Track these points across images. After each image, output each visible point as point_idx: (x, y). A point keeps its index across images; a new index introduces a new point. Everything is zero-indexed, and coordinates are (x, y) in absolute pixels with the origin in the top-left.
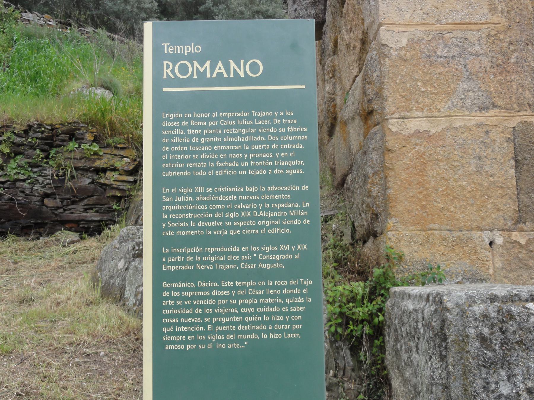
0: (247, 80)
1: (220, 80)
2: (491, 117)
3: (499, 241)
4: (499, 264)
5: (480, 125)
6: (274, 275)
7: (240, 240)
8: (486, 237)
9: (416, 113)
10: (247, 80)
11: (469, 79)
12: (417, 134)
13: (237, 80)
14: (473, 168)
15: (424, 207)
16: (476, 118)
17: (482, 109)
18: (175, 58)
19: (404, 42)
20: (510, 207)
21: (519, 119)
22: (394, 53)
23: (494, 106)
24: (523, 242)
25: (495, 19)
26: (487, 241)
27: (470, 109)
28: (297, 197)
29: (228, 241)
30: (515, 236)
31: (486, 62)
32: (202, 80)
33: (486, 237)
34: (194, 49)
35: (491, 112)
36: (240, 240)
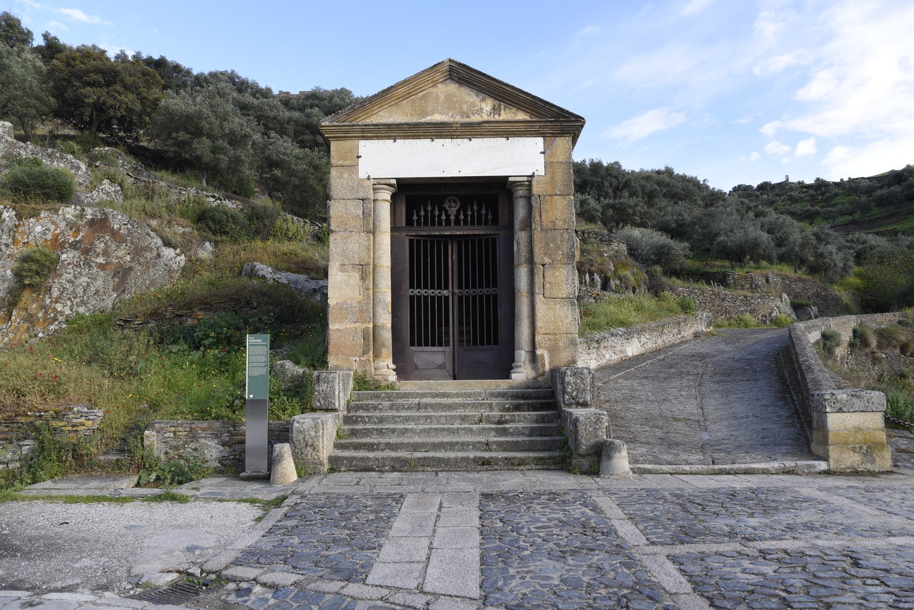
16: (353, 325)
20: (361, 350)
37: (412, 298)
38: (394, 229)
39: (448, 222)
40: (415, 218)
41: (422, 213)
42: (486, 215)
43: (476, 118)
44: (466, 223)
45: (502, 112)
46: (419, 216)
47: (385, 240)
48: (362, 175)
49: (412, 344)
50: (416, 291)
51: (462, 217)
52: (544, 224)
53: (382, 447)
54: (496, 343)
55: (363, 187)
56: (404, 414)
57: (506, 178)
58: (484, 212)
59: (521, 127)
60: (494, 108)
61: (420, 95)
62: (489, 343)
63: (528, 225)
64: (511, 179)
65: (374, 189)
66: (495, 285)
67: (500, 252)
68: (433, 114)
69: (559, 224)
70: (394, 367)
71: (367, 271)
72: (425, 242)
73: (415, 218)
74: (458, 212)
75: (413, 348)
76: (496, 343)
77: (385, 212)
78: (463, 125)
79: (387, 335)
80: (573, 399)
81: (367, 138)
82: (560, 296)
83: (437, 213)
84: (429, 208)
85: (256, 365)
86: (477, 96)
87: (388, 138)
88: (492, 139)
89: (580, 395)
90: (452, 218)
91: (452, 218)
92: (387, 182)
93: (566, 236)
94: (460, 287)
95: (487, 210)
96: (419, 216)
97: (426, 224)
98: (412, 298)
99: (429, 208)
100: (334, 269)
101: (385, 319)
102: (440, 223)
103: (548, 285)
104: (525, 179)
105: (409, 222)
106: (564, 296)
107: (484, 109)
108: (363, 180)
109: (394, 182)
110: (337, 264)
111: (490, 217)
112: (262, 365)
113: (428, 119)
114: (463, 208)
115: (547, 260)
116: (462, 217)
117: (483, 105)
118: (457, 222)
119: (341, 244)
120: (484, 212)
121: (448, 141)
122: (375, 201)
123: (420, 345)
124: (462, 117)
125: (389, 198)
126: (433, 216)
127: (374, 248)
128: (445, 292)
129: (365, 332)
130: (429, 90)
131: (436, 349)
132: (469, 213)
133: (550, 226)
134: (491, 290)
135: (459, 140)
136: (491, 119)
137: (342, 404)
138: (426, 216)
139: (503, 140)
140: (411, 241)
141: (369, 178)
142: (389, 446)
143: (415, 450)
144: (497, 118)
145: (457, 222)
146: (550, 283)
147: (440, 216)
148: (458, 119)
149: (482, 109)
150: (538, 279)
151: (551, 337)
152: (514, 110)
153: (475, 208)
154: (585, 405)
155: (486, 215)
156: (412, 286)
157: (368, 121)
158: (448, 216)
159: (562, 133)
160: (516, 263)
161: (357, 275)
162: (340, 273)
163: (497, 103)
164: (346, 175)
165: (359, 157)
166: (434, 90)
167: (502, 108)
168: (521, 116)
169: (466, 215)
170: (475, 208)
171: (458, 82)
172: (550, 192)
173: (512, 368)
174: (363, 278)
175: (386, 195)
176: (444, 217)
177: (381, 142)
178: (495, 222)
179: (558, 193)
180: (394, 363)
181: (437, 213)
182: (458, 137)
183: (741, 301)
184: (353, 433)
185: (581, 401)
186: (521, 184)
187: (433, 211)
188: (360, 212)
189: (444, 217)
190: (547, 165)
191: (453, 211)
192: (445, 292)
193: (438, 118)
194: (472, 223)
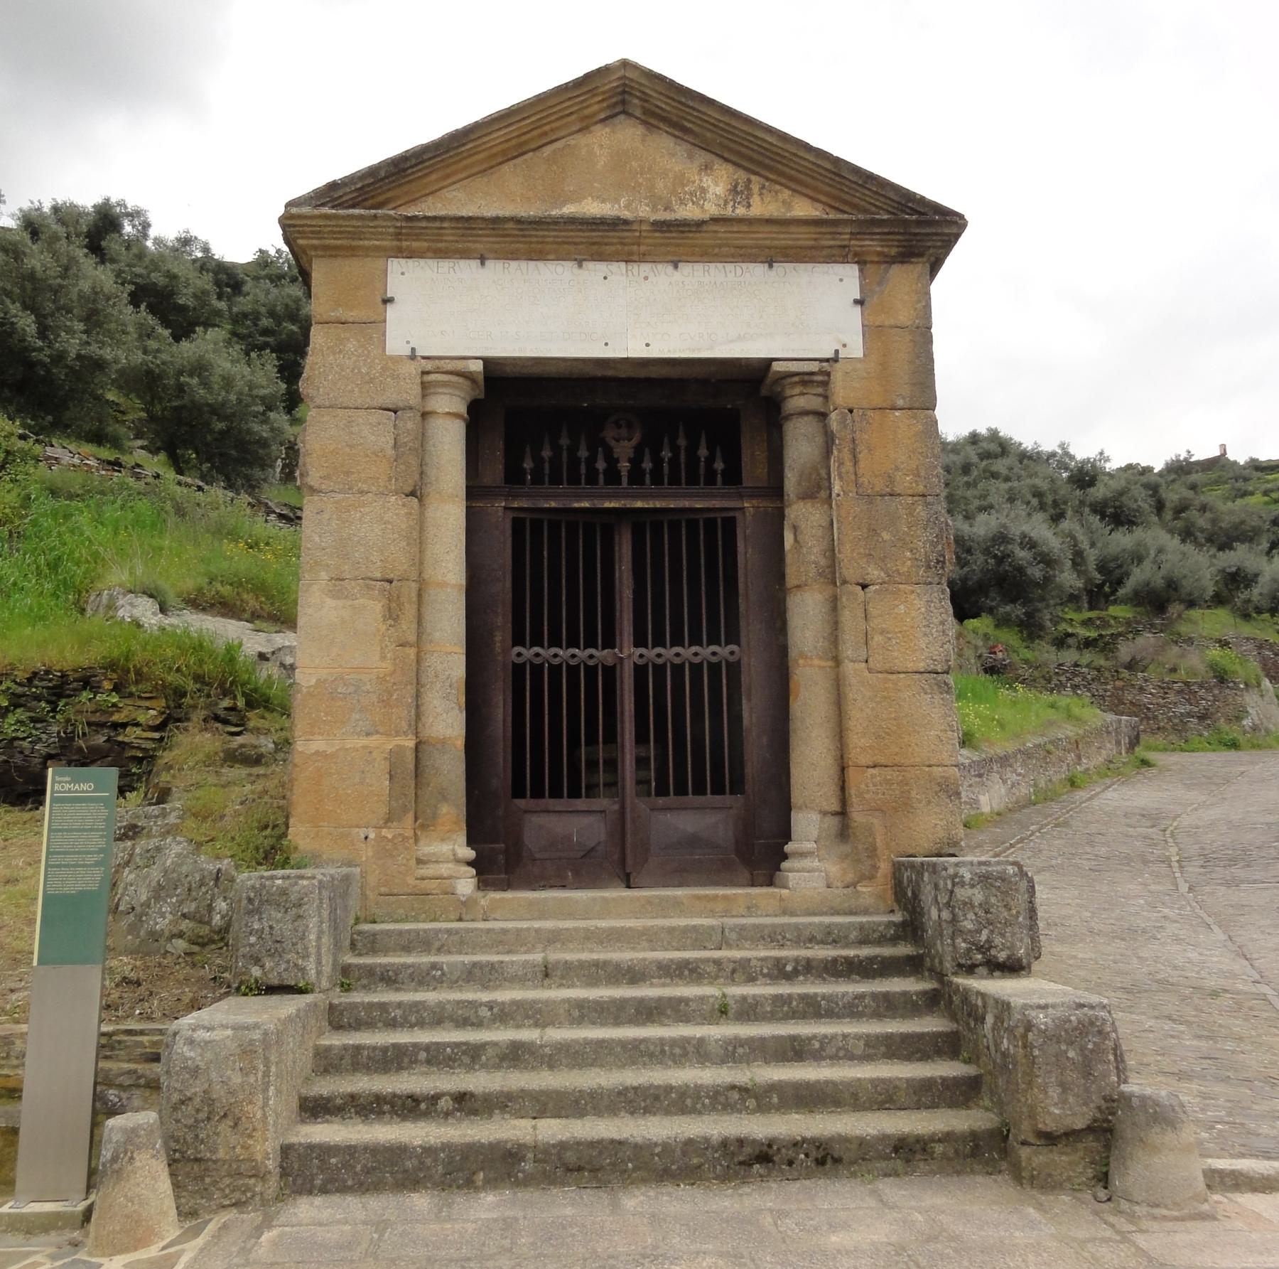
0: (87, 792)
1: (76, 791)
2: (373, 741)
3: (372, 836)
4: (370, 854)
5: (364, 747)
6: (90, 866)
7: (78, 853)
8: (362, 833)
9: (317, 737)
10: (87, 792)
11: (360, 711)
12: (317, 753)
13: (83, 792)
14: (357, 780)
15: (317, 809)
16: (364, 741)
17: (368, 734)
18: (60, 782)
19: (313, 682)
21: (395, 743)
22: (304, 690)
23: (377, 732)
24: (390, 836)
25: (384, 665)
26: (363, 836)
27: (359, 734)
28: (102, 837)
29: (74, 853)
30: (384, 832)
31: (374, 698)
32: (70, 791)
33: (362, 833)
34: (67, 779)
35: (375, 737)
36: (78, 853)
37: (518, 670)
38: (473, 492)
39: (613, 477)
40: (528, 465)
41: (547, 453)
42: (710, 460)
43: (688, 212)
44: (657, 479)
45: (755, 200)
46: (538, 461)
47: (449, 517)
48: (396, 344)
49: (518, 792)
50: (528, 653)
51: (647, 465)
52: (864, 480)
53: (444, 1103)
54: (738, 786)
55: (396, 377)
56: (505, 995)
57: (766, 364)
58: (703, 452)
59: (803, 237)
60: (734, 190)
61: (547, 151)
62: (718, 790)
63: (818, 489)
64: (776, 367)
65: (424, 385)
66: (733, 638)
67: (747, 555)
68: (577, 198)
69: (905, 482)
70: (470, 854)
71: (402, 594)
72: (554, 527)
73: (528, 465)
74: (639, 450)
75: (521, 803)
76: (738, 786)
77: (449, 445)
78: (661, 226)
79: (450, 769)
80: (980, 949)
81: (411, 255)
82: (910, 666)
83: (583, 453)
84: (564, 441)
85: (70, 859)
86: (690, 157)
87: (465, 254)
88: (729, 267)
89: (998, 940)
90: (624, 466)
91: (624, 466)
92: (460, 365)
93: (920, 511)
94: (640, 641)
95: (711, 449)
96: (538, 461)
97: (555, 480)
98: (518, 670)
99: (564, 441)
100: (315, 588)
101: (447, 722)
102: (592, 479)
103: (878, 639)
104: (814, 367)
105: (513, 476)
106: (921, 666)
107: (712, 190)
108: (397, 360)
109: (477, 367)
110: (324, 575)
111: (719, 465)
112: (90, 859)
113: (568, 210)
114: (651, 443)
115: (874, 573)
116: (647, 465)
117: (707, 181)
118: (636, 477)
119: (334, 523)
120: (703, 452)
121: (618, 268)
122: (425, 415)
123: (538, 793)
124: (655, 209)
125: (462, 409)
126: (574, 462)
127: (419, 537)
128: (602, 655)
129: (394, 758)
130: (572, 141)
131: (581, 804)
132: (666, 454)
133: (880, 485)
134: (724, 651)
135: (645, 268)
136: (729, 212)
137: (327, 969)
138: (556, 460)
139: (759, 269)
140: (518, 526)
141: (413, 357)
142: (465, 1103)
143: (540, 1114)
144: (741, 211)
145: (636, 477)
146: (882, 632)
147: (591, 461)
148: (644, 211)
149: (704, 190)
150: (850, 618)
151: (888, 773)
152: (786, 194)
153: (682, 442)
154: (1013, 968)
155: (710, 460)
156: (518, 640)
157: (412, 211)
158: (612, 462)
159: (907, 255)
160: (791, 580)
161: (376, 607)
162: (330, 602)
163: (742, 175)
164: (351, 346)
165: (387, 301)
166: (582, 140)
167: (755, 188)
168: (803, 209)
169: (658, 461)
170: (682, 442)
171: (645, 123)
172: (878, 401)
173: (785, 857)
174: (392, 615)
175: (450, 404)
176: (601, 465)
177: (445, 265)
178: (733, 476)
179: (900, 403)
180: (471, 842)
181: (583, 453)
182: (643, 258)
183: (1180, 692)
184: (358, 1060)
185: (1002, 956)
186: (805, 379)
187: (573, 449)
188: (386, 441)
189: (601, 465)
190: (871, 332)
191: (624, 450)
192: (602, 655)
193: (592, 208)
194: (675, 480)
